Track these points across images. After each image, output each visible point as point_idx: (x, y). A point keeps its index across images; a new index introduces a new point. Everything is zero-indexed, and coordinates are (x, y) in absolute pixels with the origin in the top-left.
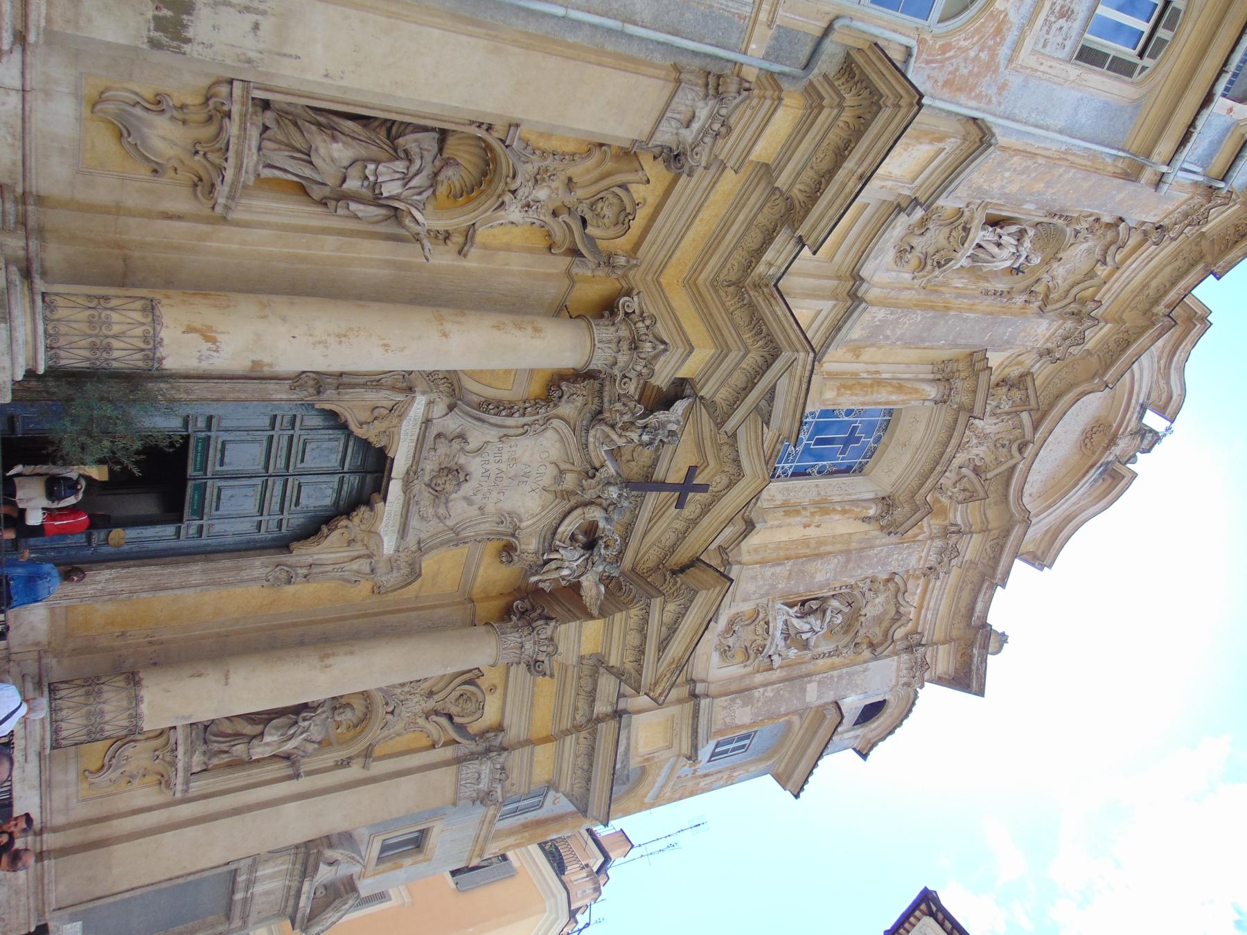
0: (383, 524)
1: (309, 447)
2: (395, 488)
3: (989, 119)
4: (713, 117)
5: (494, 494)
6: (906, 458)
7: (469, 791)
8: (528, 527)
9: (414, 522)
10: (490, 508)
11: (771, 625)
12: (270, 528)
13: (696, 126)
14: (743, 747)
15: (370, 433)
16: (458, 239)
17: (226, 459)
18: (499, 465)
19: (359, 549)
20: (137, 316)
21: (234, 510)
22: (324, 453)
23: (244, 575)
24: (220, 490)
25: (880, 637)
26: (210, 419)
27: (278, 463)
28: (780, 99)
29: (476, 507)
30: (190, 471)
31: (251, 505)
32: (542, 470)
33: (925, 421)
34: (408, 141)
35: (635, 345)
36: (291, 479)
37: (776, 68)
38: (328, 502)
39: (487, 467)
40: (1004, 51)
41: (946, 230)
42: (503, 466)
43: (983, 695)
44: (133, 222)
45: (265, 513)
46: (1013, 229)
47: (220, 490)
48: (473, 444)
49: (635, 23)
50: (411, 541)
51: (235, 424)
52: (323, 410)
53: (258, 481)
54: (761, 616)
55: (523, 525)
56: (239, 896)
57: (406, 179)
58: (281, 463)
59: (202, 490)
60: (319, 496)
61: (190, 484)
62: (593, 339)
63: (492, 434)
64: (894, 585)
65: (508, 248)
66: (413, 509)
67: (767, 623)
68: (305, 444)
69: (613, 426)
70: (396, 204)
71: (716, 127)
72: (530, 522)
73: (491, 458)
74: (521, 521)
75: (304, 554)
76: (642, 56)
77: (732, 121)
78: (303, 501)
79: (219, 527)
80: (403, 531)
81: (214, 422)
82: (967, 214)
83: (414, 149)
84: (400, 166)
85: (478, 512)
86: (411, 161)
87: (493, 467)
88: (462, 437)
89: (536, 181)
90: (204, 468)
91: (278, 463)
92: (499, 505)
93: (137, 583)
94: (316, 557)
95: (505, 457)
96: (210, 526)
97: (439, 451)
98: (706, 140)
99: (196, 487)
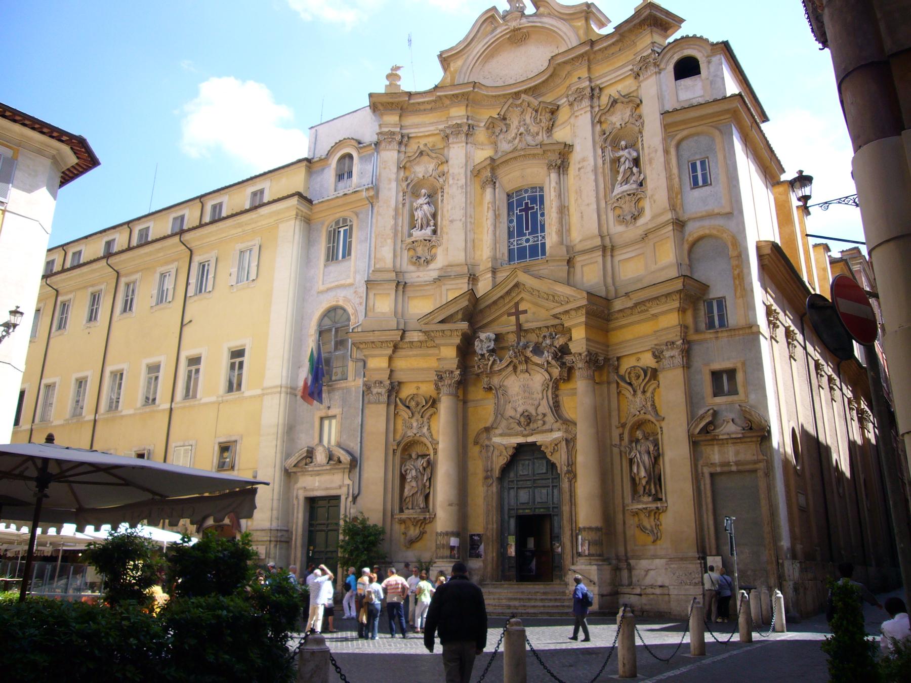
1: (521, 473)
2: (530, 439)
4: (375, 387)
9: (547, 427)
13: (380, 390)
14: (703, 163)
25: (631, 105)
31: (544, 491)
38: (544, 462)
40: (351, 290)
48: (512, 413)
54: (615, 205)
56: (734, 468)
58: (528, 483)
63: (509, 407)
75: (562, 467)
78: (544, 471)
80: (551, 430)
87: (521, 402)
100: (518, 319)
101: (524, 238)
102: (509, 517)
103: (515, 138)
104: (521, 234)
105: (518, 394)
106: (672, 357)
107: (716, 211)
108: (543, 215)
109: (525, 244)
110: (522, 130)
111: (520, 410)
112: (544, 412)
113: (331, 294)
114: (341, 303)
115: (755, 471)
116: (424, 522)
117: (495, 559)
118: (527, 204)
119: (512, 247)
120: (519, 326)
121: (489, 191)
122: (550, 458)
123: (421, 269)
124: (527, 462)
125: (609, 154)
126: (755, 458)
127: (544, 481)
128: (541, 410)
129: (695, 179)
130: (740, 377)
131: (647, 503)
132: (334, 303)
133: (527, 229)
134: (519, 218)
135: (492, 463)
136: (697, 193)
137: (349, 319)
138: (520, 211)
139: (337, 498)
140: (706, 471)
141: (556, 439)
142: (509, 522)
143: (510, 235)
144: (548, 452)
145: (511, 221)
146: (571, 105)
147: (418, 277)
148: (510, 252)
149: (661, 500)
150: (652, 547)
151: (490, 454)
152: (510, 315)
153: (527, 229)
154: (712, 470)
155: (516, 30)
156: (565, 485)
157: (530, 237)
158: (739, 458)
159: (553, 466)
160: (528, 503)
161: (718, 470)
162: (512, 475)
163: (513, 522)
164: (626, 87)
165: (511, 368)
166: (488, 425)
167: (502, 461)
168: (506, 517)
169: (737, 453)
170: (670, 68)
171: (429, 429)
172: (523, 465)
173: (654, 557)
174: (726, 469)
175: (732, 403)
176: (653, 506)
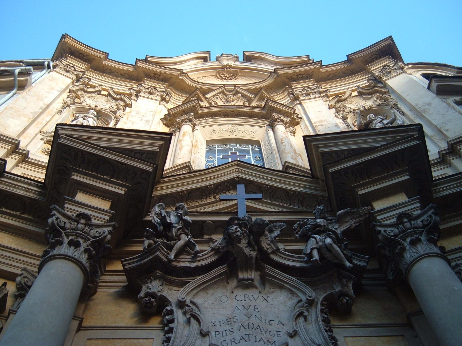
5: (270, 328)
6: (240, 127)
8: (304, 293)
10: (289, 328)
18: (235, 330)
25: (377, 94)
29: (290, 341)
39: (238, 338)
42: (236, 327)
43: (391, 37)
69: (170, 248)
74: (300, 301)
85: (297, 339)
92: (285, 322)
95: (228, 328)
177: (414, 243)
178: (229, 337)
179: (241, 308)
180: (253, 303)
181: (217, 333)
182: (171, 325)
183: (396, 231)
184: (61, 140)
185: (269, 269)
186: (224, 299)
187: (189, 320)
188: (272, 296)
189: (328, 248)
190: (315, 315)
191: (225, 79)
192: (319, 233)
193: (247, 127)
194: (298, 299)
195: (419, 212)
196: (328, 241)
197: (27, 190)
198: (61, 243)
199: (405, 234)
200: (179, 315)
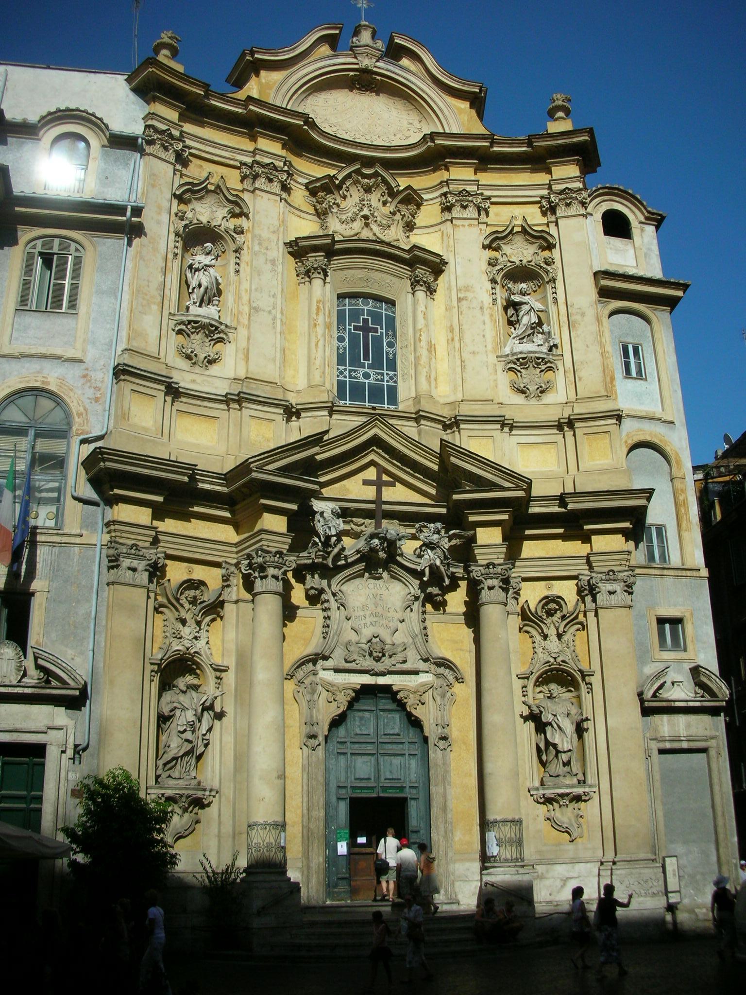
0: (409, 684)
1: (359, 732)
2: (382, 681)
3: (112, 366)
4: (128, 555)
5: (389, 615)
7: (621, 597)
10: (400, 616)
11: (519, 356)
12: (417, 750)
14: (636, 350)
15: (343, 700)
16: (218, 674)
17: (366, 777)
19: (427, 697)
20: (254, 832)
21: (399, 770)
22: (364, 723)
23: (440, 762)
24: (386, 779)
26: (339, 787)
27: (370, 748)
28: (114, 521)
29: (399, 624)
30: (374, 795)
31: (396, 761)
32: (371, 586)
33: (345, 272)
34: (166, 711)
35: (262, 568)
36: (381, 740)
37: (100, 524)
38: (397, 716)
41: (192, 336)
42: (368, 613)
44: (223, 830)
45: (403, 752)
46: (189, 275)
47: (386, 779)
48: (353, 637)
49: (91, 612)
50: (422, 666)
51: (343, 774)
52: (329, 730)
53: (381, 759)
55: (412, 591)
56: (685, 745)
57: (184, 709)
58: (369, 747)
59: (384, 789)
60: (394, 723)
61: (382, 795)
62: (263, 593)
64: (494, 242)
65: (223, 641)
66: (399, 667)
67: (518, 359)
68: (357, 734)
69: (329, 553)
70: (200, 710)
71: (133, 551)
72: (410, 587)
73: (363, 621)
76: (105, 604)
77: (130, 542)
78: (396, 731)
79: (413, 777)
80: (416, 673)
81: (341, 785)
82: (179, 327)
83: (170, 707)
84: (178, 712)
86: (175, 708)
87: (368, 620)
88: (348, 644)
89: (180, 638)
90: (372, 788)
91: (370, 748)
92: (398, 610)
93: (441, 820)
94: (432, 721)
95: (362, 613)
96: (410, 782)
97: (355, 657)
98: (141, 553)
99: (383, 791)
100: (379, 492)
101: (362, 371)
102: (339, 799)
103: (353, 220)
104: (355, 362)
105: (364, 607)
106: (610, 593)
107: (657, 416)
108: (391, 345)
109: (362, 380)
110: (366, 212)
111: (367, 633)
112: (406, 641)
113: (33, 366)
114: (53, 388)
115: (704, 750)
116: (199, 803)
117: (321, 867)
118: (366, 321)
119: (341, 378)
120: (378, 501)
121: (317, 282)
122: (414, 712)
123: (197, 369)
124: (367, 714)
125: (501, 295)
126: (708, 733)
127: (394, 746)
128: (399, 638)
129: (627, 365)
130: (689, 627)
131: (568, 786)
132: (38, 384)
133: (366, 357)
134: (353, 339)
135: (318, 710)
136: (631, 384)
137: (69, 424)
138: (356, 328)
139: (39, 750)
140: (655, 746)
141: (423, 685)
142: (337, 808)
143: (341, 360)
144: (410, 702)
145: (341, 339)
146: (447, 209)
147: (194, 381)
148: (341, 385)
149: (584, 782)
150: (571, 847)
151: (316, 697)
152: (366, 483)
153: (366, 357)
154: (662, 746)
155: (365, 71)
156: (435, 755)
157: (371, 372)
158: (689, 733)
159: (416, 723)
160: (369, 779)
161: (668, 745)
162: (342, 731)
163: (343, 808)
164: (535, 217)
165: (362, 566)
166: (310, 649)
167: (334, 710)
168: (334, 799)
169: (688, 726)
170: (598, 216)
171: (207, 643)
172: (361, 718)
173: (574, 861)
174: (676, 745)
175: (681, 661)
176: (579, 790)
177: (491, 588)
178: (363, 621)
179: (371, 596)
180: (379, 592)
181: (356, 617)
182: (329, 613)
183: (483, 572)
184: (253, 474)
185: (395, 568)
186: (361, 586)
187: (338, 608)
188: (392, 585)
189: (438, 567)
190: (417, 605)
191: (359, 89)
192: (432, 549)
193: (383, 275)
194: (407, 591)
195: (501, 561)
196: (438, 562)
197: (212, 483)
198: (266, 577)
199: (488, 576)
200: (333, 604)
